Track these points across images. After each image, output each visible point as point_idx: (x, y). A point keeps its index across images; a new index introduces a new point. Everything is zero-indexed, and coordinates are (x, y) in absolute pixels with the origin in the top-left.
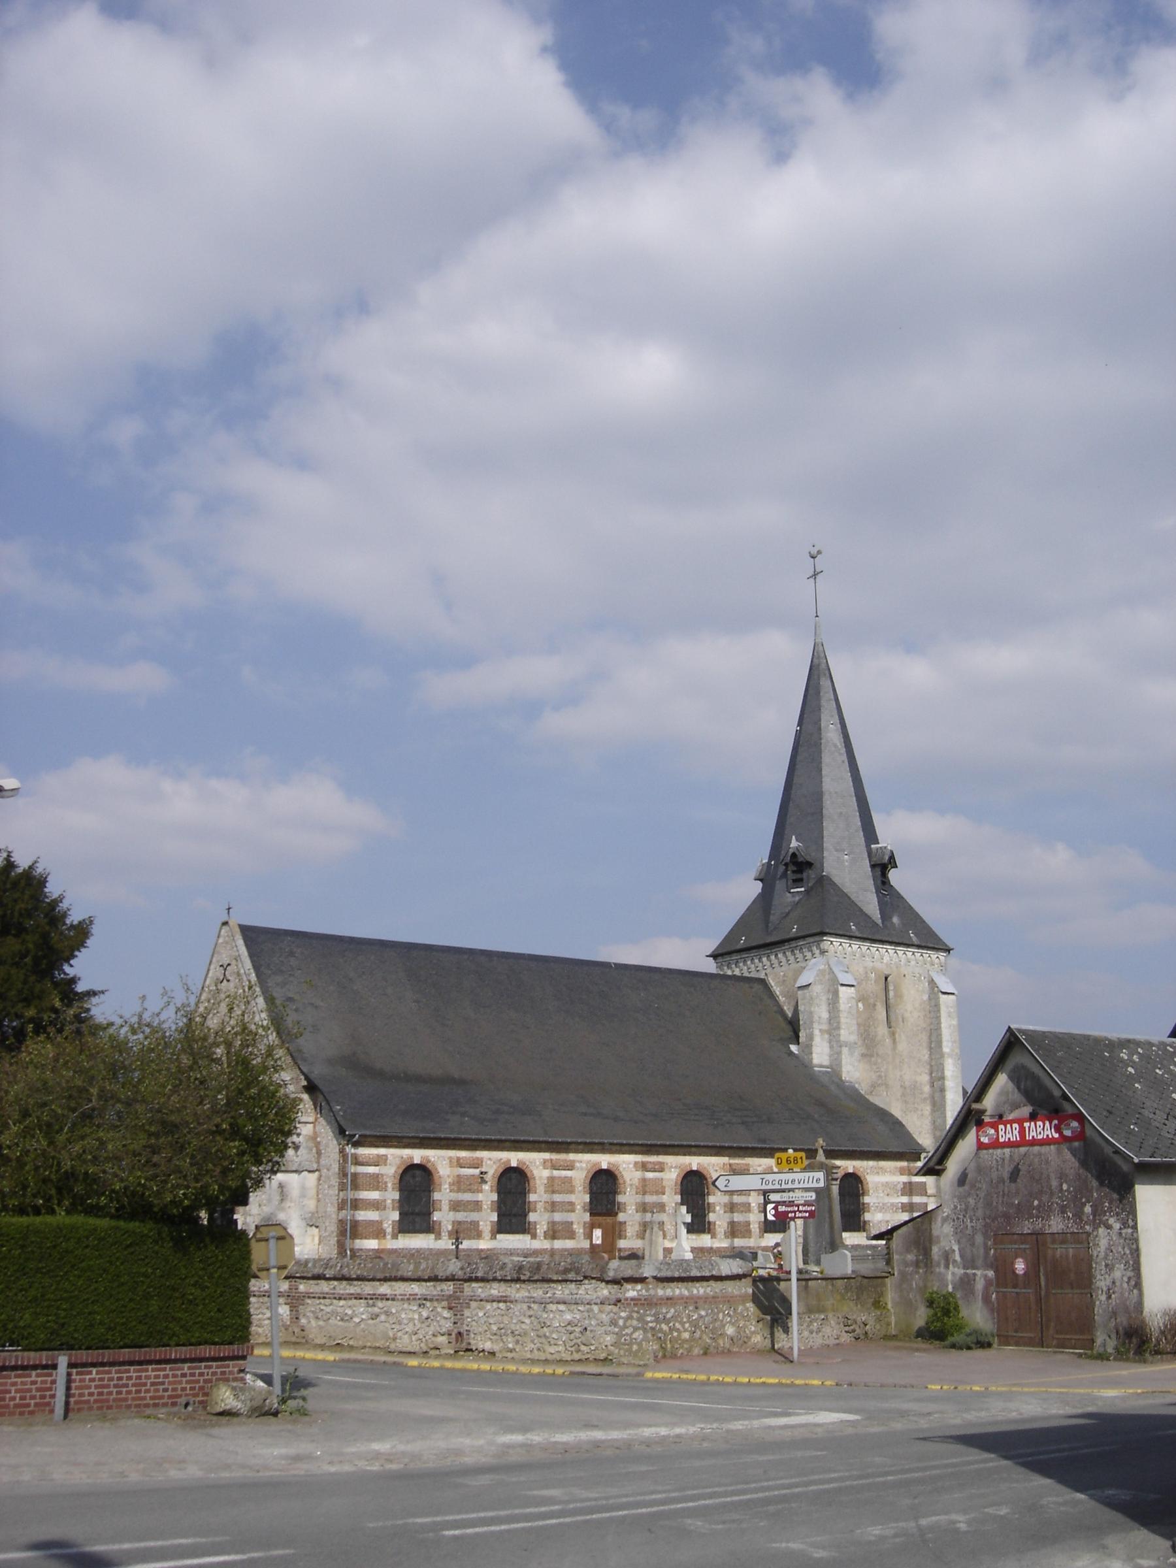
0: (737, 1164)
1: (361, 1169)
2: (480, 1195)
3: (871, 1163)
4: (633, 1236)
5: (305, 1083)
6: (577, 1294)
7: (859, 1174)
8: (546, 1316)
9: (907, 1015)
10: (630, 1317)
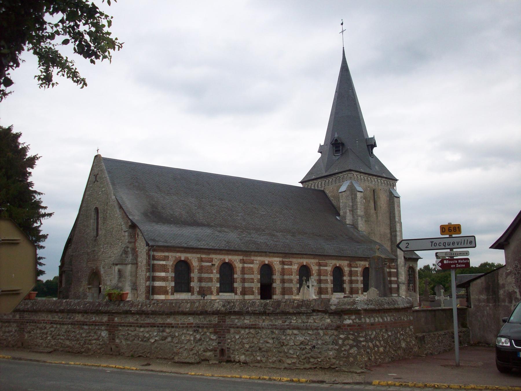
0: (323, 263)
1: (156, 262)
2: (212, 275)
4: (279, 294)
5: (130, 224)
6: (307, 322)
8: (284, 338)
9: (382, 205)
10: (347, 338)
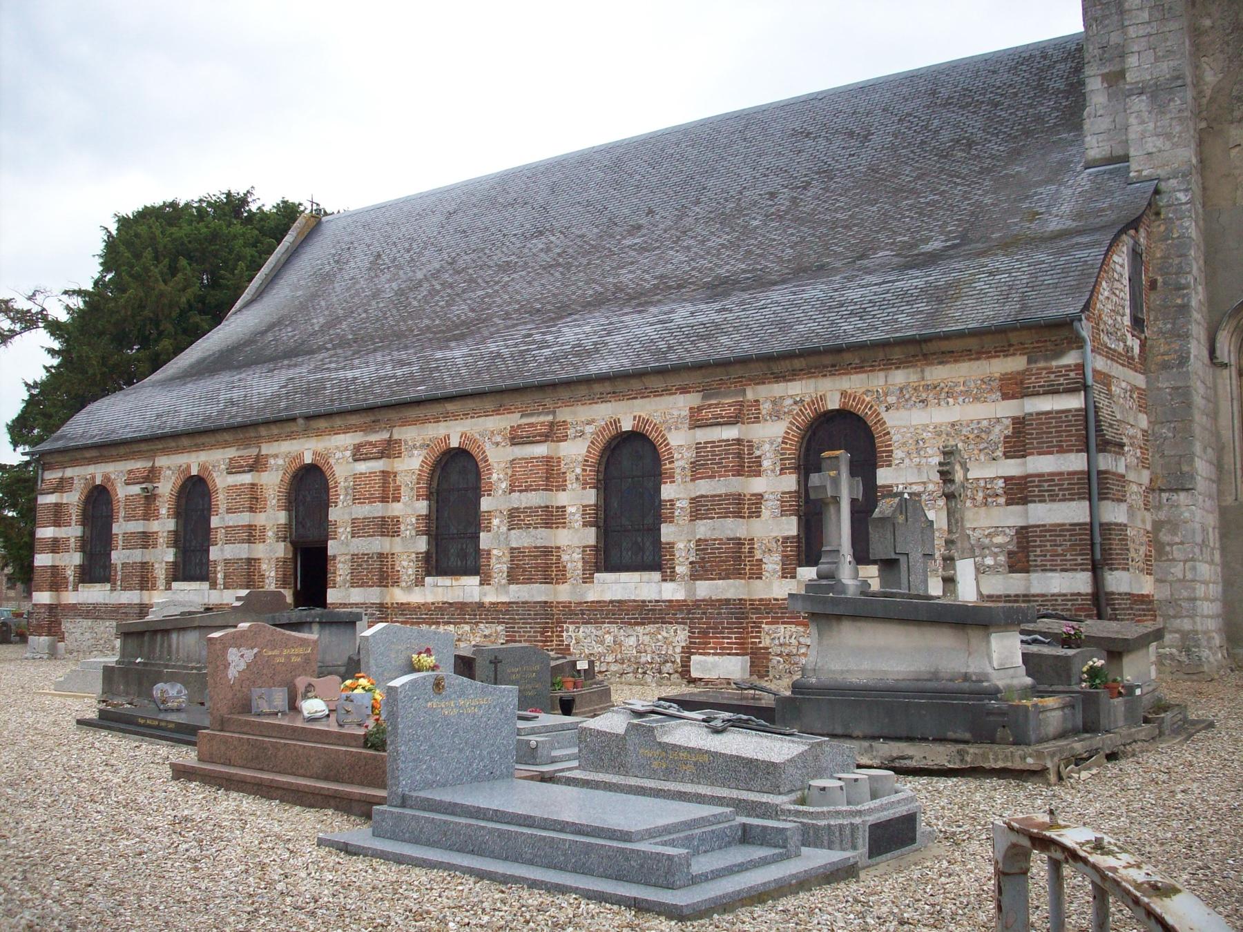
3: (899, 377)
4: (345, 582)
7: (860, 410)
